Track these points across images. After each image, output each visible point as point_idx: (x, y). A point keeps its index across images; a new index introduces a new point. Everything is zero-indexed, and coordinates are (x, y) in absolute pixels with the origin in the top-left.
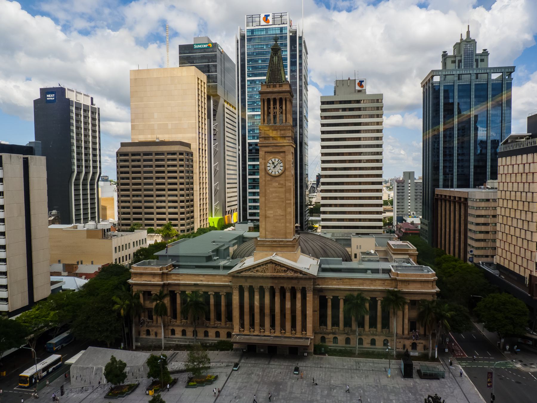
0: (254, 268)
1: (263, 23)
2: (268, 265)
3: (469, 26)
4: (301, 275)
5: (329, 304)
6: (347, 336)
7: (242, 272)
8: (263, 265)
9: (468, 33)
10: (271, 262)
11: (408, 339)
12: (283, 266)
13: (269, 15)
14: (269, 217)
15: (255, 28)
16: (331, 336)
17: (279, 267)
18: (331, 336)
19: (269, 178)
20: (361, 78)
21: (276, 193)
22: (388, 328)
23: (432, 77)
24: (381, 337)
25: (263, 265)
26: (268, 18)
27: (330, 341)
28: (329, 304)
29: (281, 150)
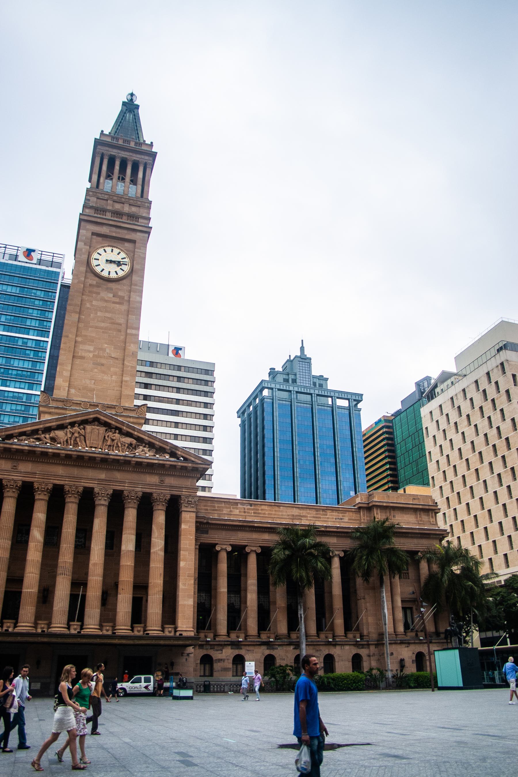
0: (48, 430)
1: (22, 258)
2: (89, 428)
3: (302, 341)
4: (176, 460)
5: (223, 566)
6: (267, 652)
7: (10, 437)
8: (72, 424)
9: (302, 349)
10: (96, 421)
11: (408, 643)
12: (129, 435)
13: (34, 251)
14: (83, 358)
15: (6, 262)
16: (228, 653)
17: (117, 435)
18: (228, 653)
19: (94, 281)
20: (179, 345)
21: (106, 311)
22: (358, 629)
23: (263, 388)
24: (347, 647)
25: (72, 424)
26: (32, 254)
27: (226, 669)
28: (223, 566)
29: (127, 237)
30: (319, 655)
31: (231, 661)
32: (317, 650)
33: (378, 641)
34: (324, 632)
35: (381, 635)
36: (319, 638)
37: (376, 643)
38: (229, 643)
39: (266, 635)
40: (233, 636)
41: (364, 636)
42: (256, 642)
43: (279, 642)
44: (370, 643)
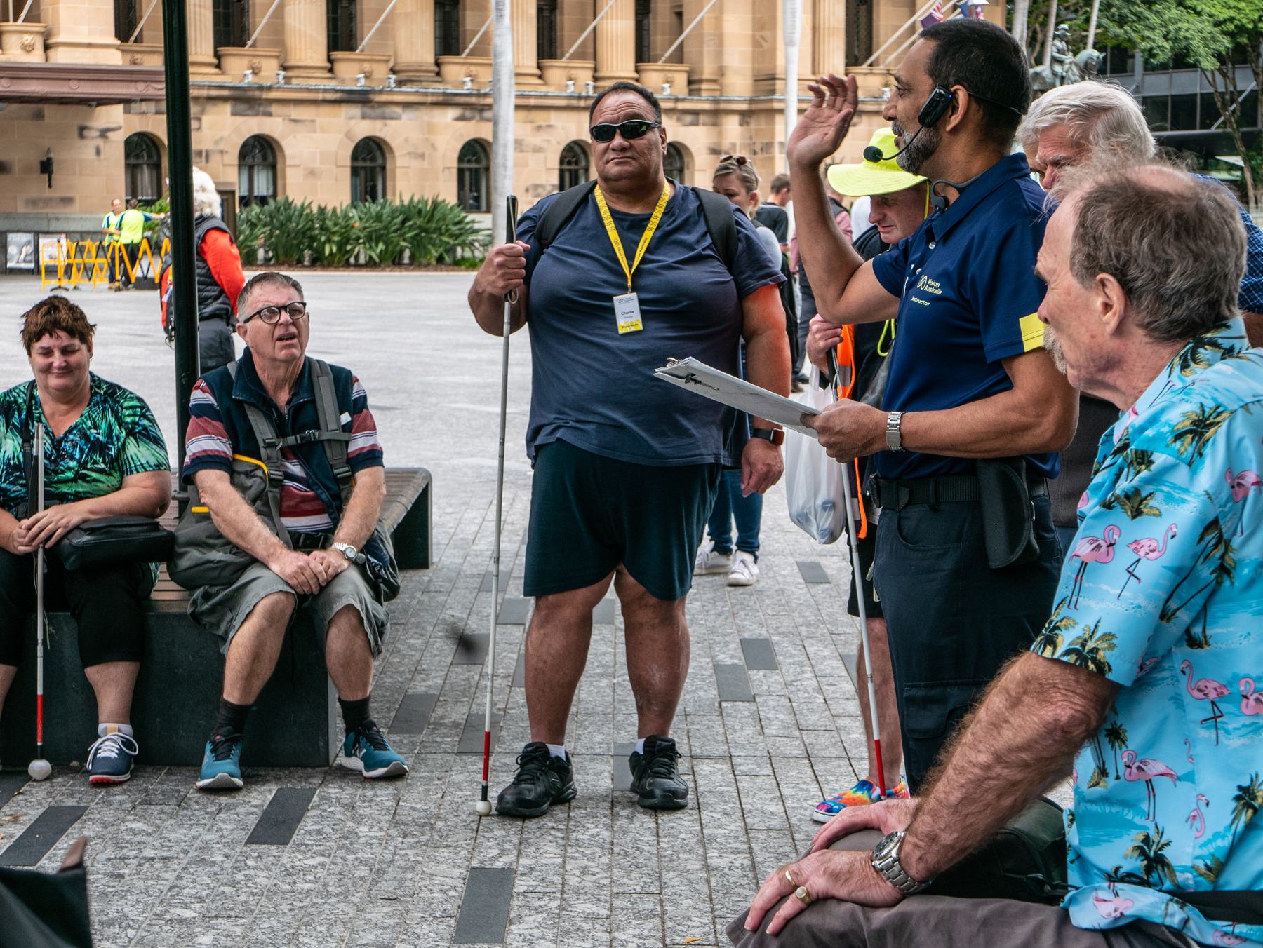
6: (365, 128)
30: (544, 145)
31: (233, 158)
32: (539, 127)
33: (751, 101)
34: (562, 62)
35: (766, 81)
36: (545, 84)
37: (744, 107)
38: (225, 93)
39: (356, 66)
40: (238, 69)
41: (701, 81)
42: (325, 91)
43: (409, 93)
44: (723, 106)
